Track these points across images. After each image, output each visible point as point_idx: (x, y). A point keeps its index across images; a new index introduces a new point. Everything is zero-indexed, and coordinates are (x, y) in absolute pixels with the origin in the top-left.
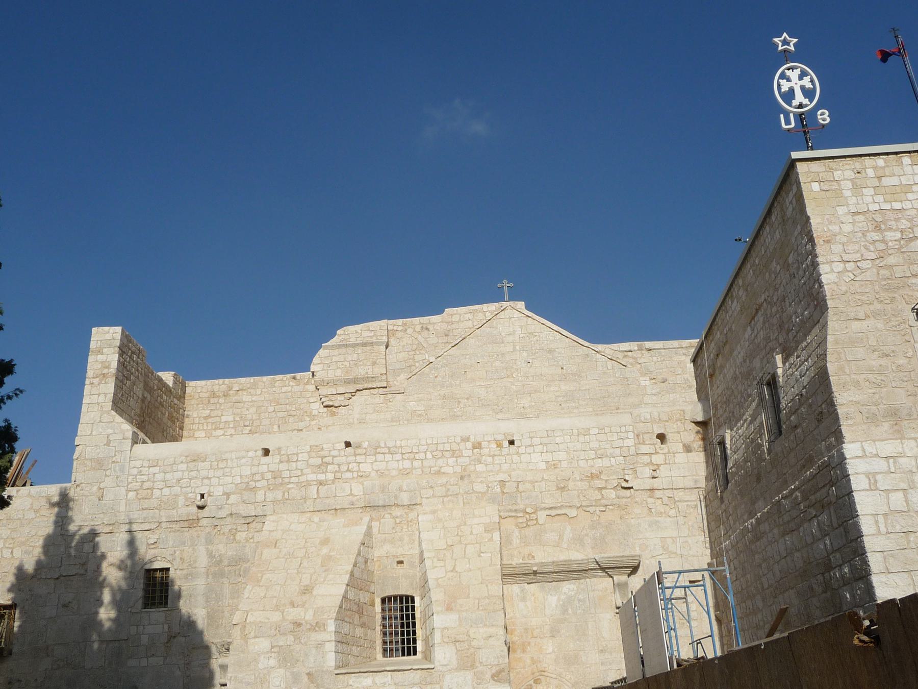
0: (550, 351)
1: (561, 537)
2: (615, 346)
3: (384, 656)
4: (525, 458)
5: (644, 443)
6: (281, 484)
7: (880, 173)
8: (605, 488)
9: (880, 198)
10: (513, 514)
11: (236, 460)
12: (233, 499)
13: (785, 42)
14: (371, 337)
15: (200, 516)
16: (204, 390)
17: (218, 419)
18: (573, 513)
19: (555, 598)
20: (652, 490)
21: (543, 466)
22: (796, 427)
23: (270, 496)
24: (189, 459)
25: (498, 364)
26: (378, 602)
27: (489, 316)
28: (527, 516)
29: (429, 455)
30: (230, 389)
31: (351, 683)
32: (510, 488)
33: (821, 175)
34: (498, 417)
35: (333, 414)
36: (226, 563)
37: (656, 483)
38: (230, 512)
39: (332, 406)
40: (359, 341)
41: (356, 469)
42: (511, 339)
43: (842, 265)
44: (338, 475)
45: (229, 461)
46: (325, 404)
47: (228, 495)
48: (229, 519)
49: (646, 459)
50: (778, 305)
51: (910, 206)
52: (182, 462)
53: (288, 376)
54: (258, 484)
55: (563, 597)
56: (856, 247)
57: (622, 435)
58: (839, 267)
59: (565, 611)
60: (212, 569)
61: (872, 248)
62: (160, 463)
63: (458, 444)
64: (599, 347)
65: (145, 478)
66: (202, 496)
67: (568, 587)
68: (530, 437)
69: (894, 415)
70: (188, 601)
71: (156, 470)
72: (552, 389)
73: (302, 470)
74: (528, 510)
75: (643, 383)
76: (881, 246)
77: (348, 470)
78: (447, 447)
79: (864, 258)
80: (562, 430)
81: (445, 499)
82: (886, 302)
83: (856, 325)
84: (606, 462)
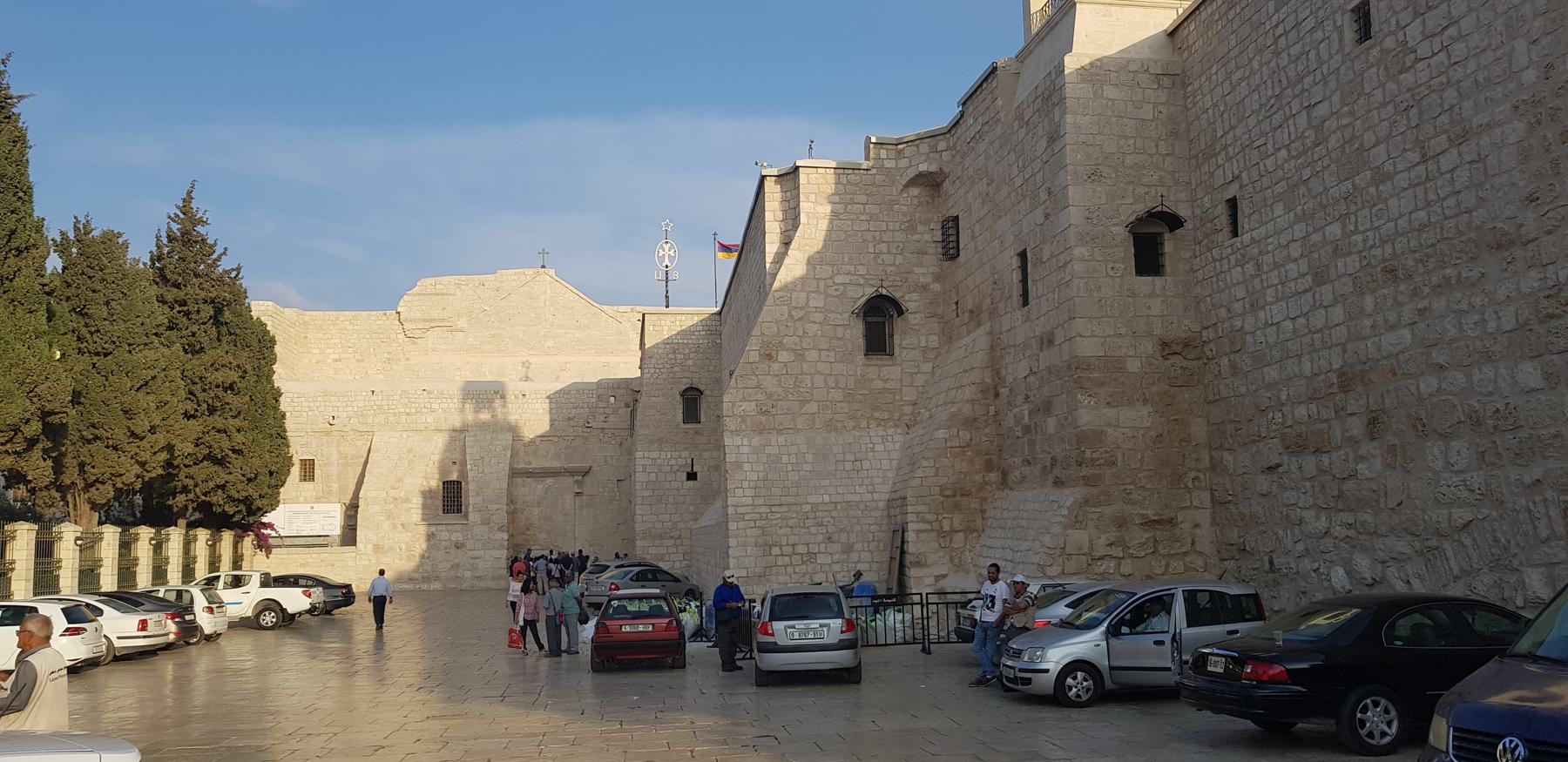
1: (548, 453)
3: (444, 513)
14: (443, 290)
18: (556, 439)
19: (541, 486)
20: (603, 429)
25: (532, 314)
34: (531, 352)
35: (414, 343)
36: (349, 458)
37: (606, 425)
44: (419, 410)
49: (602, 410)
53: (381, 312)
58: (652, 371)
59: (546, 493)
60: (341, 461)
64: (605, 308)
65: (296, 404)
67: (549, 481)
71: (303, 400)
75: (631, 336)
76: (673, 362)
83: (653, 399)
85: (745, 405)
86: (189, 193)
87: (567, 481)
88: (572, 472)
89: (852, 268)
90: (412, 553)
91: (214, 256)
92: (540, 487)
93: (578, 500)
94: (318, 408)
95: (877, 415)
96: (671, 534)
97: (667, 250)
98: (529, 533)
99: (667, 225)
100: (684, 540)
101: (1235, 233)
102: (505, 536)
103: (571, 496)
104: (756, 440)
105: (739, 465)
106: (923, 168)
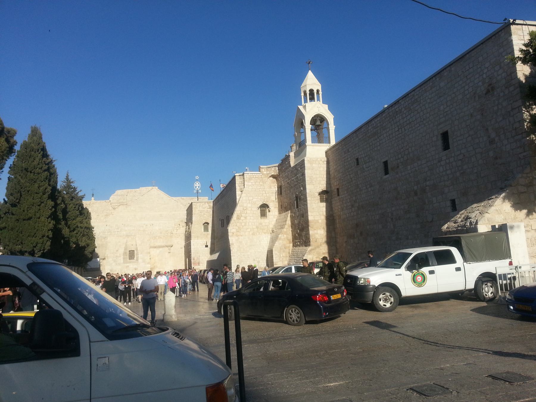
0: (162, 198)
2: (176, 198)
12: (101, 234)
13: (197, 177)
20: (176, 233)
21: (158, 229)
26: (128, 251)
27: (150, 190)
29: (138, 227)
30: (90, 203)
35: (114, 210)
40: (121, 194)
47: (100, 233)
53: (104, 201)
58: (195, 218)
64: (173, 198)
67: (161, 249)
69: (198, 237)
85: (234, 230)
86: (67, 174)
89: (257, 197)
91: (77, 192)
92: (158, 251)
95: (264, 231)
97: (197, 184)
99: (197, 178)
101: (338, 195)
104: (236, 238)
105: (233, 244)
106: (273, 174)
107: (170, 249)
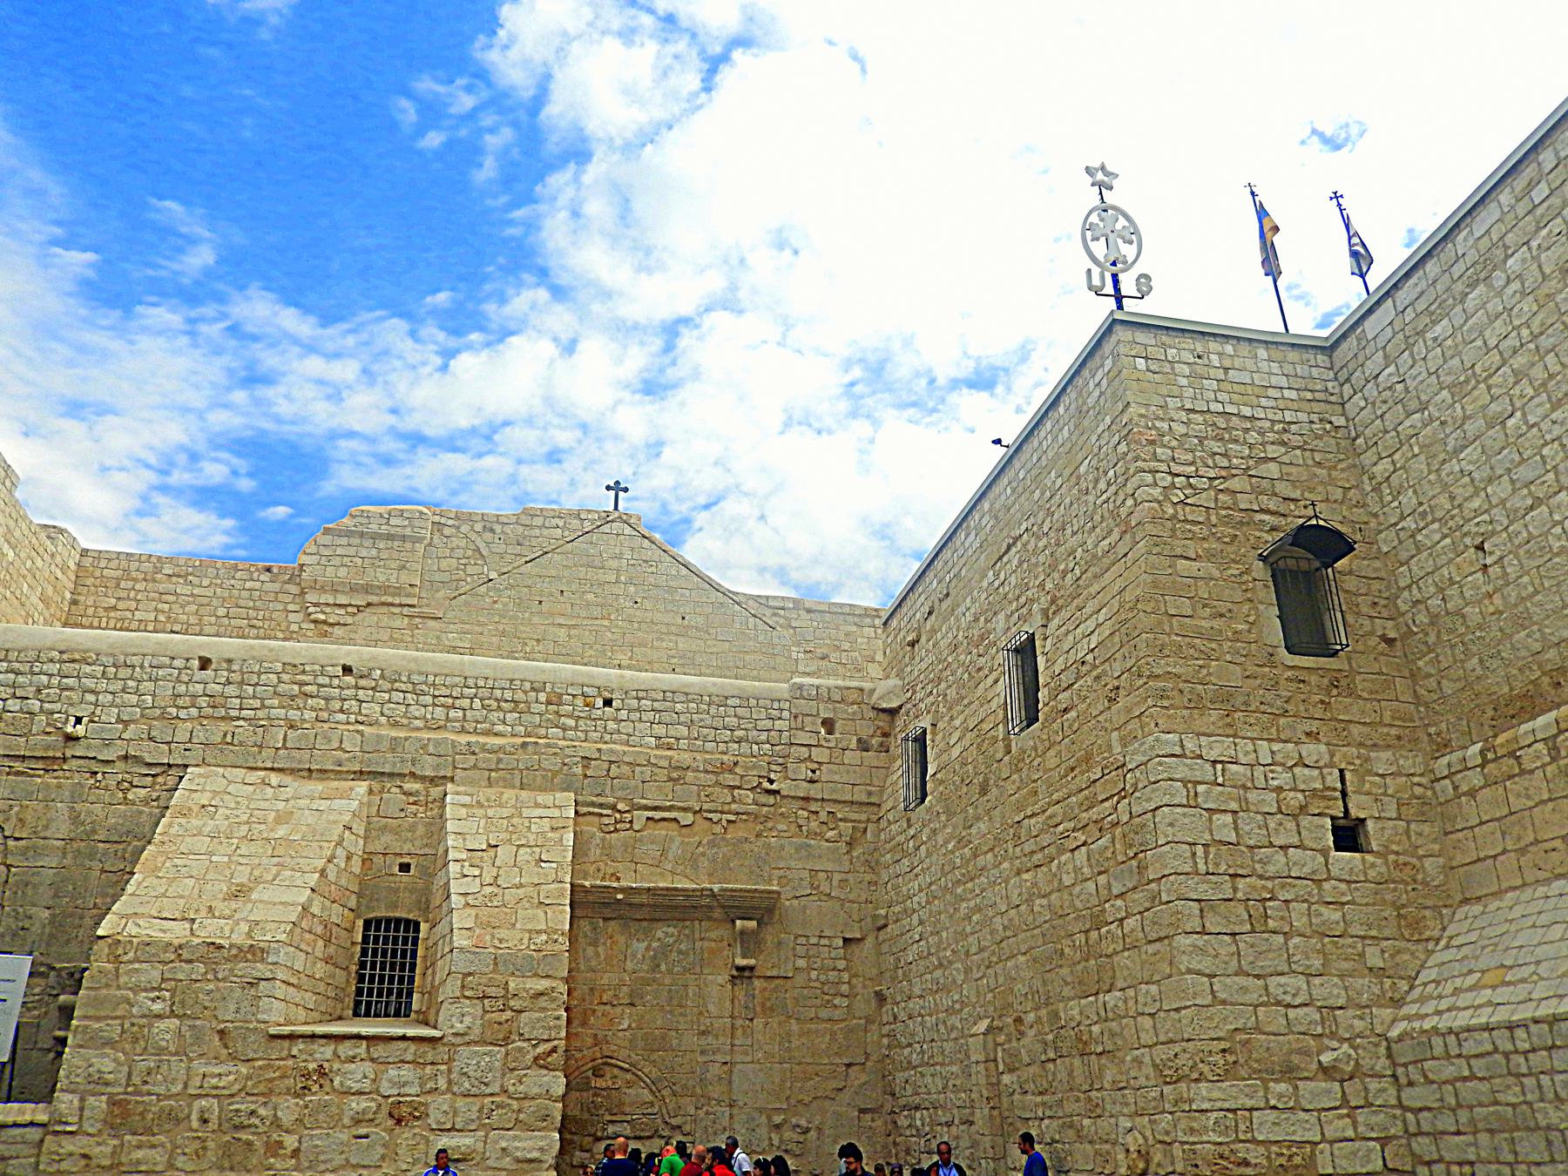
0: (672, 590)
1: (664, 852)
4: (626, 727)
5: (802, 729)
6: (223, 718)
7: (1227, 363)
8: (739, 788)
9: (1222, 396)
10: (596, 810)
11: (149, 670)
15: (69, 753)
16: (114, 564)
17: (129, 615)
18: (687, 819)
20: (806, 799)
22: (1066, 710)
23: (200, 736)
24: (65, 657)
27: (588, 526)
28: (618, 816)
29: (477, 703)
31: (294, 1052)
32: (596, 769)
33: (1149, 349)
37: (815, 790)
38: (124, 753)
39: (325, 622)
41: (355, 709)
42: (614, 564)
43: (1169, 478)
44: (325, 715)
45: (138, 669)
46: (312, 617)
47: (126, 723)
48: (120, 765)
50: (1052, 534)
51: (1263, 416)
52: (51, 661)
54: (183, 714)
55: (655, 944)
56: (1189, 457)
57: (774, 712)
61: (1210, 463)
62: (13, 656)
63: (525, 692)
66: (79, 721)
68: (637, 698)
70: (20, 892)
72: (664, 644)
73: (262, 699)
74: (621, 806)
75: (794, 655)
77: (342, 711)
78: (508, 695)
79: (1200, 473)
80: (687, 694)
81: (493, 774)
82: (1226, 540)
84: (745, 746)
87: (713, 935)
88: (732, 907)
90: (244, 1136)
93: (740, 992)
94: (39, 691)
96: (1326, 1058)
98: (600, 1083)
100: (1373, 1085)
102: (558, 1084)
103: (723, 978)
107: (749, 942)
